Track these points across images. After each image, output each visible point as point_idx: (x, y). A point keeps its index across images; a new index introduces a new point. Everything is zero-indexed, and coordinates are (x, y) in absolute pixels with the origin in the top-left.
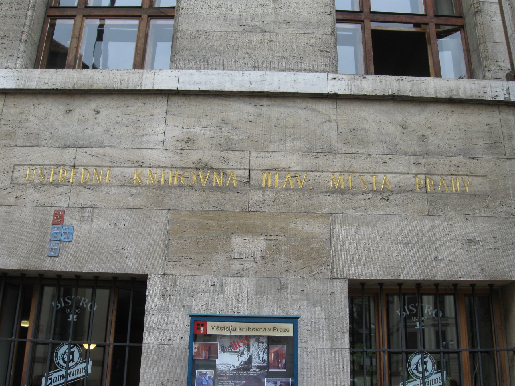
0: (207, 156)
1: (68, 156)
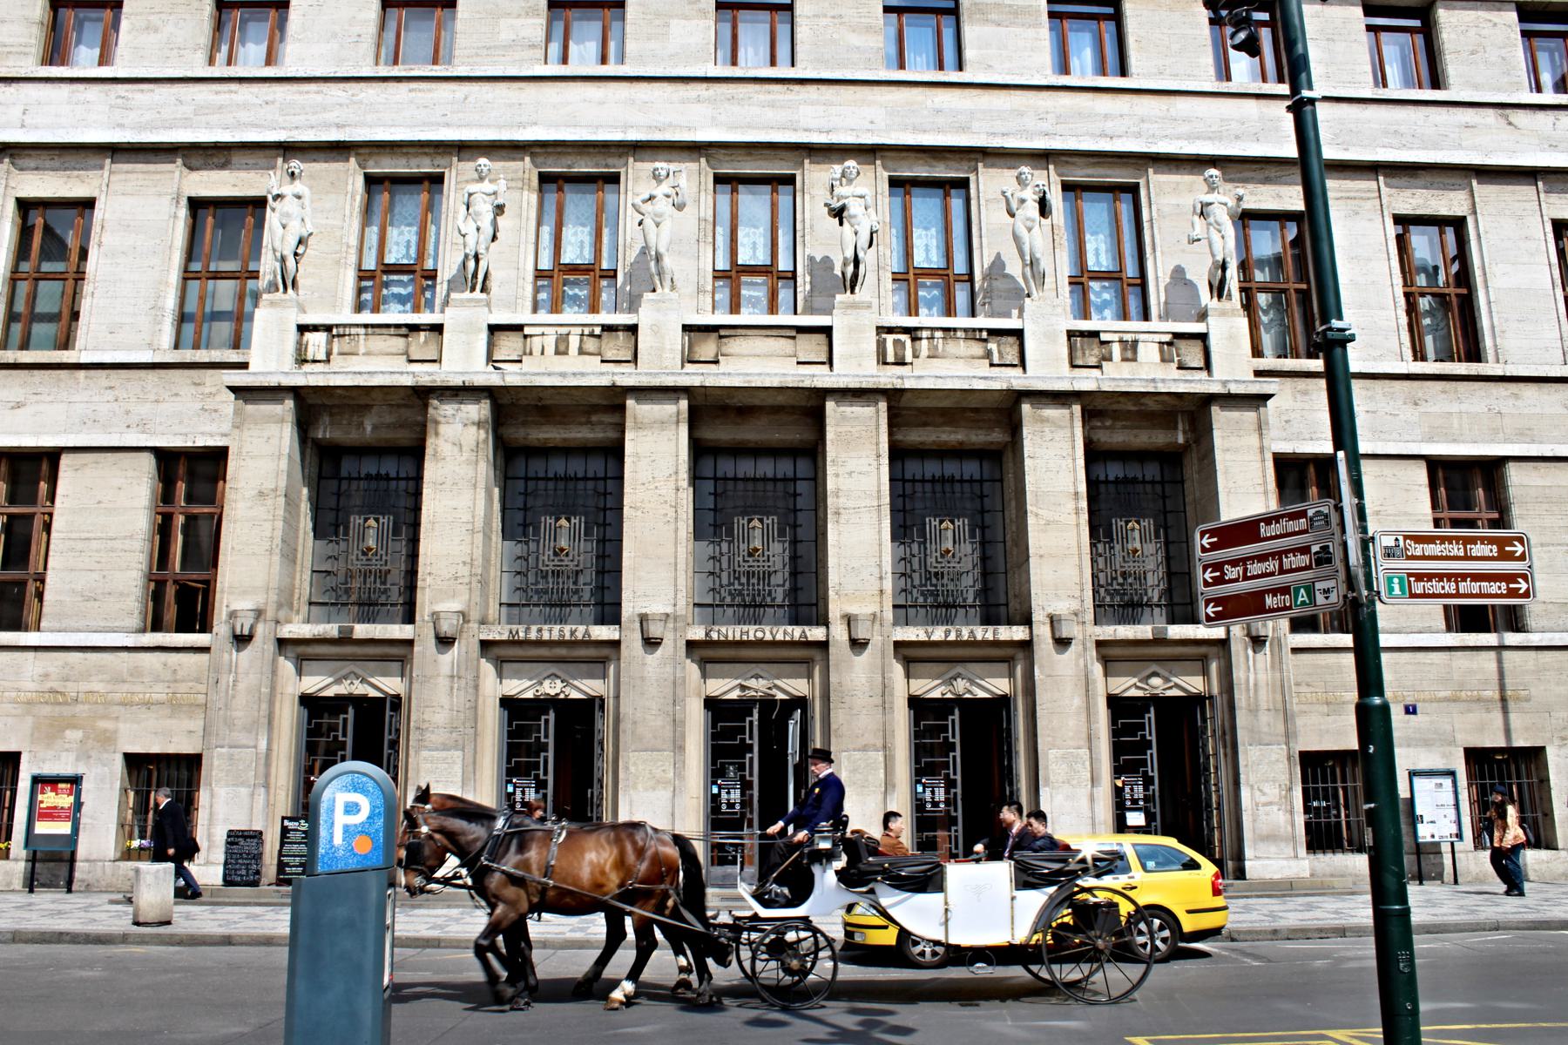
0: (56, 685)
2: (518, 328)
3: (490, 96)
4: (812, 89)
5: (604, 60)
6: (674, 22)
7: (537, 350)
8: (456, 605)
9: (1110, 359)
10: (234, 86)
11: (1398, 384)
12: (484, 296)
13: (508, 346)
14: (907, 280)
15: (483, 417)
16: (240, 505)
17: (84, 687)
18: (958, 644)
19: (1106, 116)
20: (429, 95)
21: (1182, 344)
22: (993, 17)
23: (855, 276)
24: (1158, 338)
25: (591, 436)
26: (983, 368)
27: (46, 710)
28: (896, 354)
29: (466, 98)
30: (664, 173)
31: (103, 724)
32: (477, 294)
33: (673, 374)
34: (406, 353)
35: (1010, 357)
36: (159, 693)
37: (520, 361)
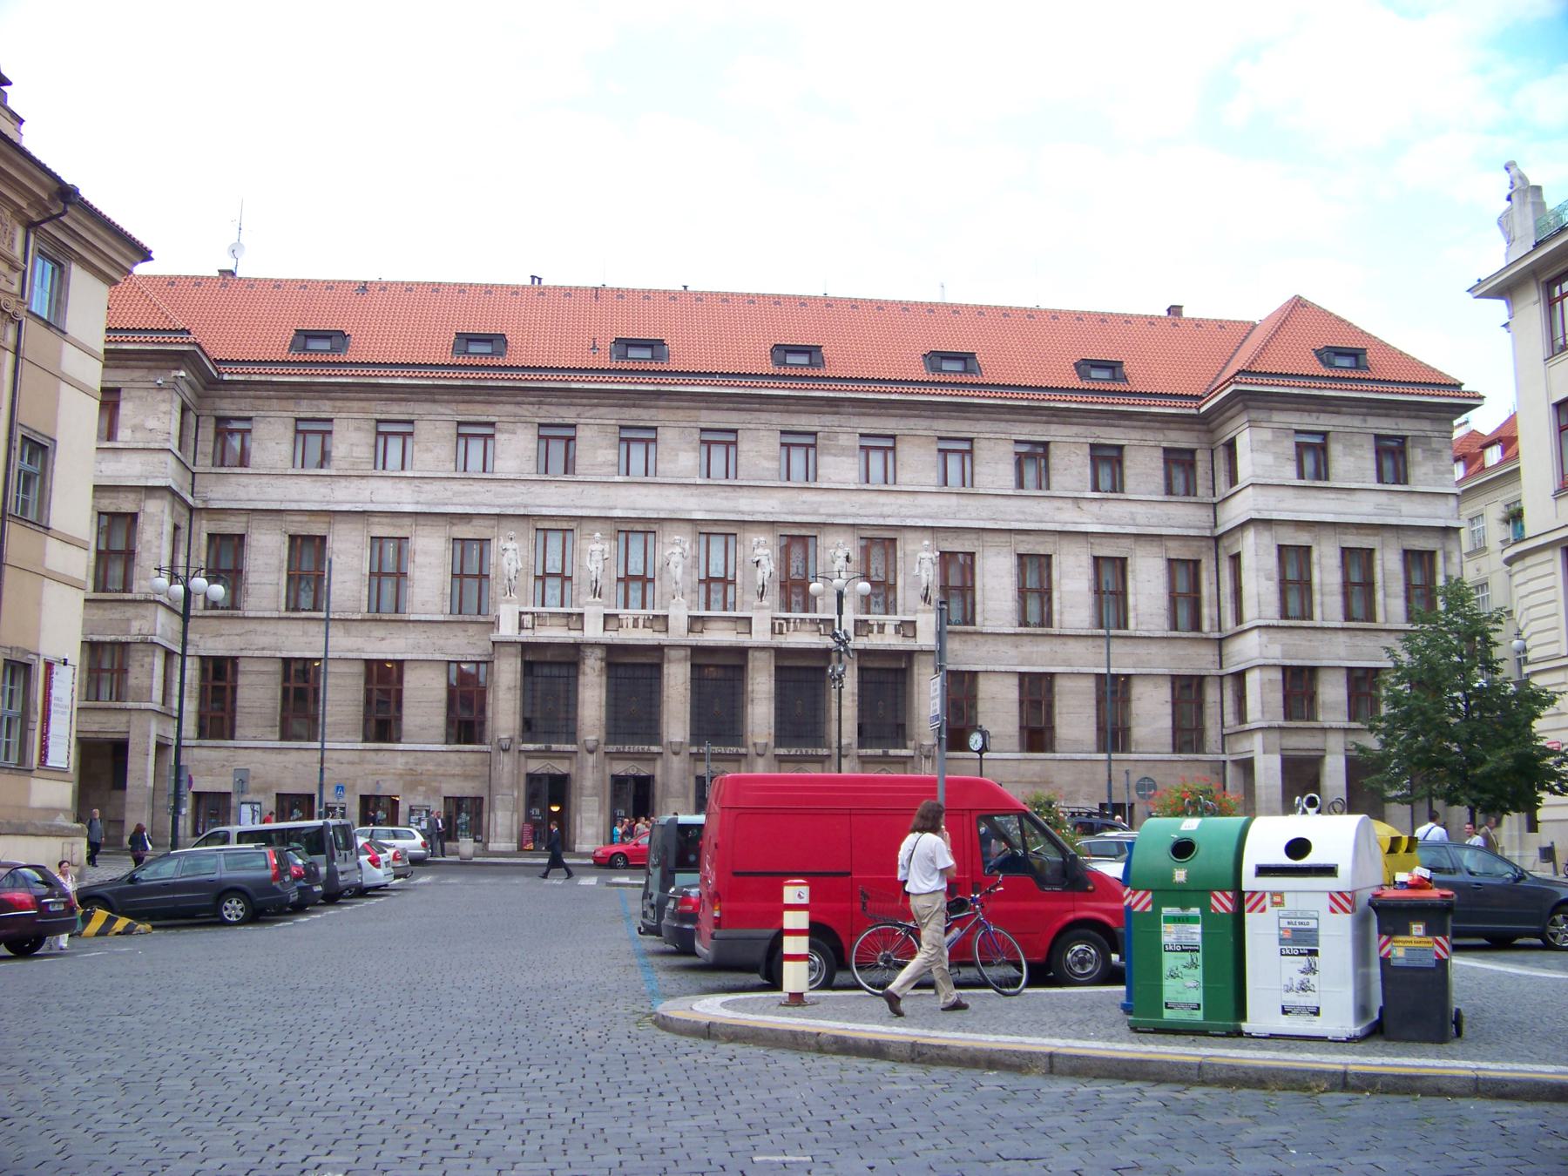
1: (380, 766)
2: (617, 615)
3: (594, 492)
4: (745, 490)
6: (681, 454)
8: (594, 738)
9: (872, 632)
10: (471, 482)
11: (1009, 638)
13: (613, 624)
16: (500, 693)
17: (424, 767)
18: (801, 755)
19: (883, 505)
21: (905, 626)
22: (833, 451)
23: (763, 591)
24: (894, 623)
27: (409, 778)
31: (434, 784)
32: (597, 598)
34: (567, 625)
36: (458, 770)
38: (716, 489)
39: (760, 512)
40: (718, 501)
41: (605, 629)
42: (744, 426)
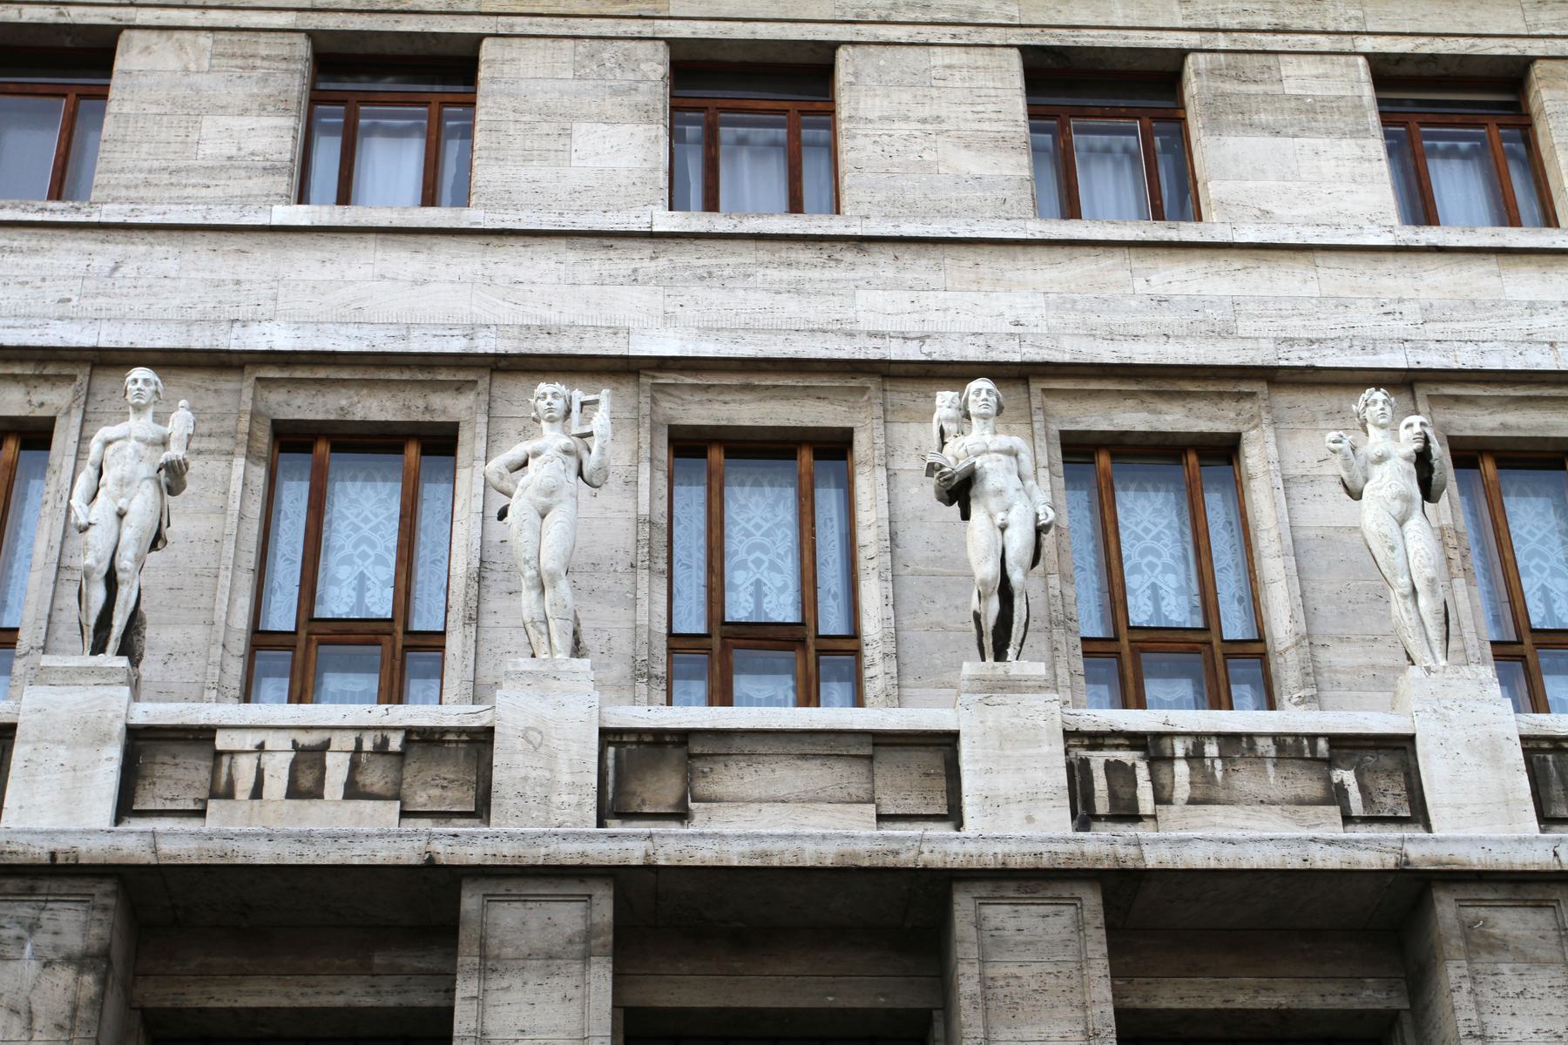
2: (202, 736)
3: (171, 266)
5: (430, 198)
7: (245, 782)
12: (124, 662)
14: (1118, 655)
15: (95, 946)
19: (1532, 306)
20: (38, 260)
25: (369, 1001)
26: (1328, 823)
28: (1113, 796)
29: (115, 269)
30: (559, 404)
33: (577, 836)
35: (1389, 801)
37: (201, 814)
38: (747, 255)
39: (963, 335)
40: (761, 299)
41: (125, 808)
42: (867, 33)
